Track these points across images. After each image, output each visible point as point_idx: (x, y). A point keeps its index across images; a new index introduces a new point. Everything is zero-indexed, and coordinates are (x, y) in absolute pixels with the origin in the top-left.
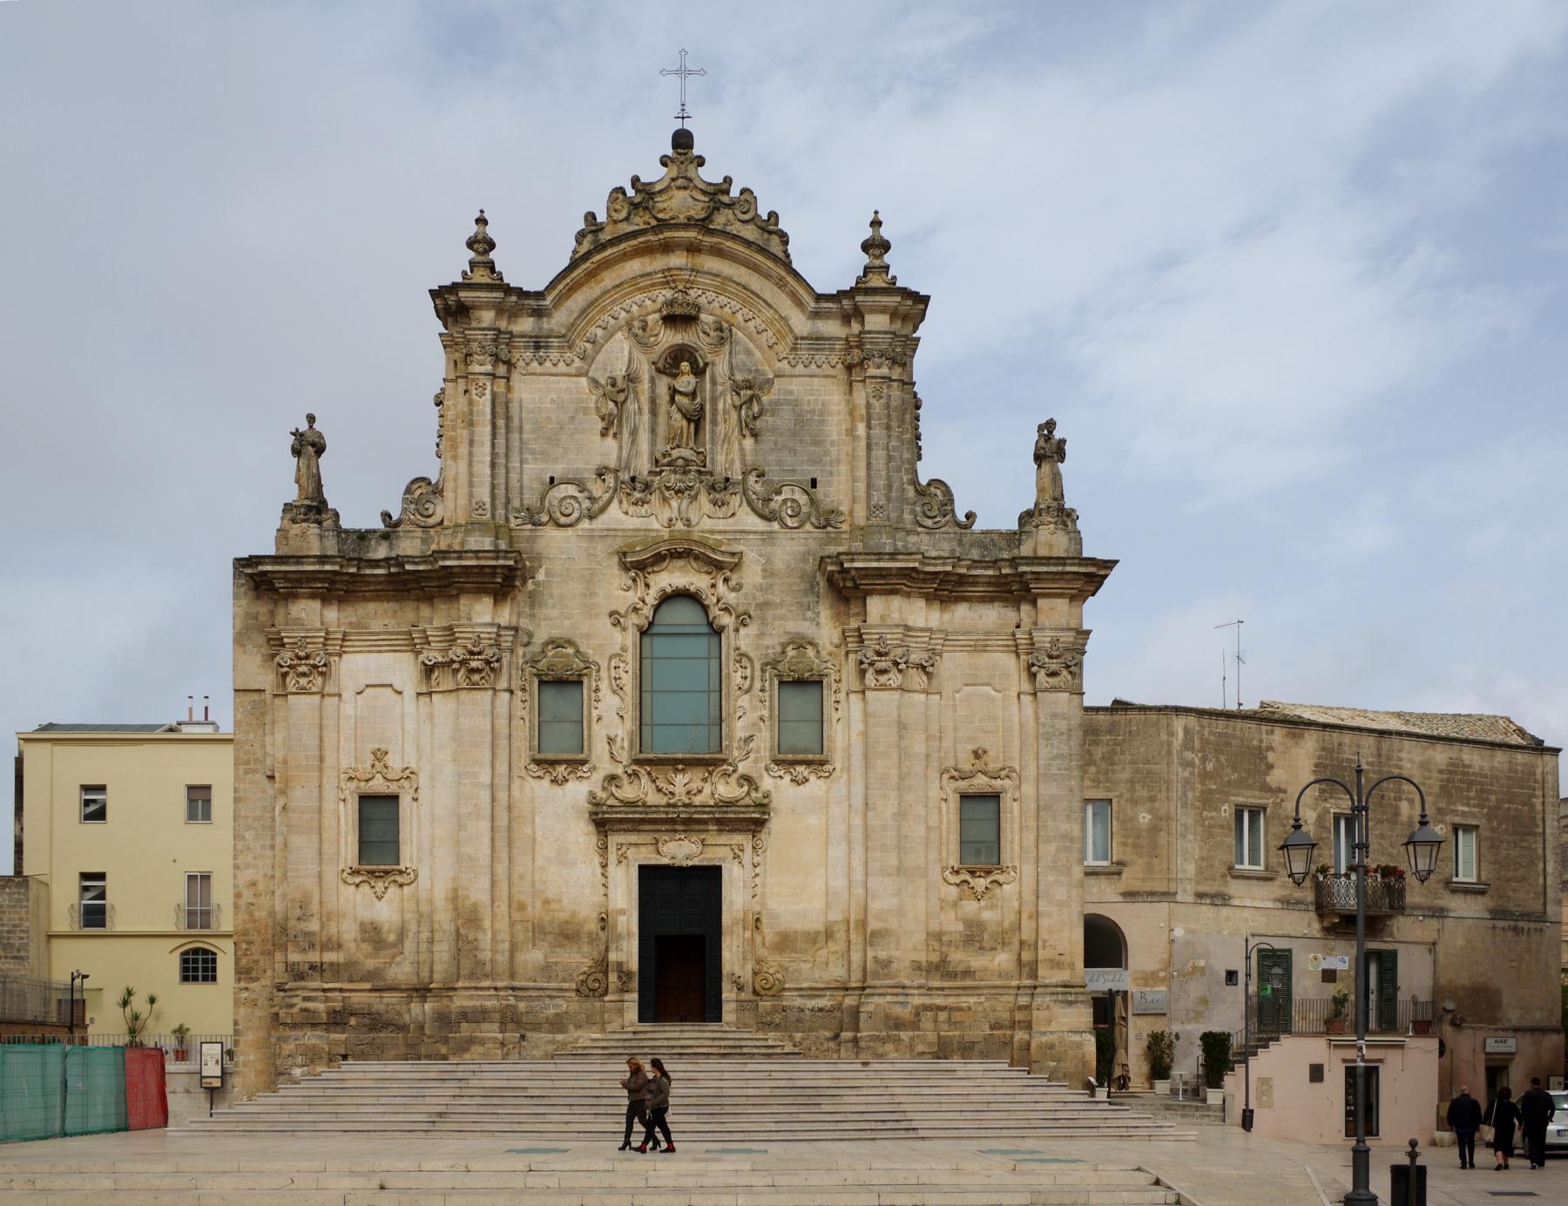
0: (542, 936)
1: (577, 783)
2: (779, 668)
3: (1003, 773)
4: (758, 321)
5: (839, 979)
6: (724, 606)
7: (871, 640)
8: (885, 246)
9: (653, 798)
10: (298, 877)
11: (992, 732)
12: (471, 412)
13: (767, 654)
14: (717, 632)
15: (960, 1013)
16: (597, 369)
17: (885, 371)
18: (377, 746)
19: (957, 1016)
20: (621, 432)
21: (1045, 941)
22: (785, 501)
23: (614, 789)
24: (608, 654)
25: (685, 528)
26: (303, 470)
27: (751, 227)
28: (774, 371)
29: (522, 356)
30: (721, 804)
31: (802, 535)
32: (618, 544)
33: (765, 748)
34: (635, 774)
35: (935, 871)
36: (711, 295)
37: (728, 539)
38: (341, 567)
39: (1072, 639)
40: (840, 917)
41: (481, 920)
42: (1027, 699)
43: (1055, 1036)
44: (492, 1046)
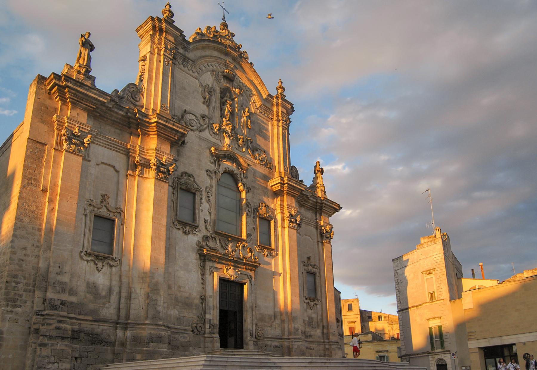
0: (177, 303)
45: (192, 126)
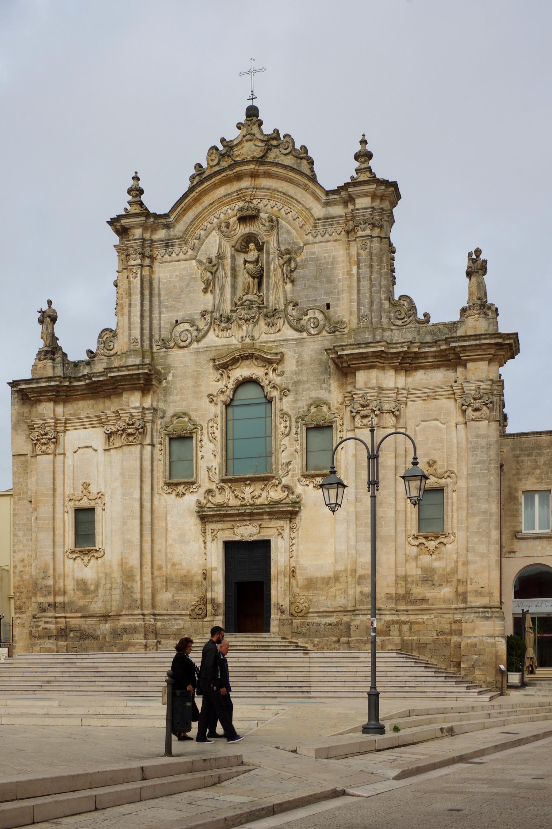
0: (171, 585)
1: (190, 495)
2: (306, 420)
3: (446, 475)
4: (293, 213)
5: (342, 605)
6: (273, 385)
7: (358, 398)
8: (369, 156)
9: (233, 502)
10: (43, 555)
11: (439, 449)
12: (130, 288)
13: (299, 412)
14: (270, 401)
15: (418, 625)
16: (201, 254)
17: (368, 232)
18: (84, 481)
19: (415, 627)
20: (215, 290)
21: (472, 579)
22: (309, 319)
23: (210, 498)
24: (207, 419)
25: (251, 341)
26: (45, 331)
27: (290, 157)
28: (303, 242)
29: (159, 252)
30: (272, 503)
31: (320, 339)
32: (212, 355)
33: (298, 468)
34: (222, 488)
35: (402, 537)
36: (265, 201)
37: (276, 346)
38: (61, 382)
39: (489, 387)
40: (343, 568)
41: (134, 576)
42: (461, 427)
43: (477, 639)
44: (139, 647)
45: (185, 341)
